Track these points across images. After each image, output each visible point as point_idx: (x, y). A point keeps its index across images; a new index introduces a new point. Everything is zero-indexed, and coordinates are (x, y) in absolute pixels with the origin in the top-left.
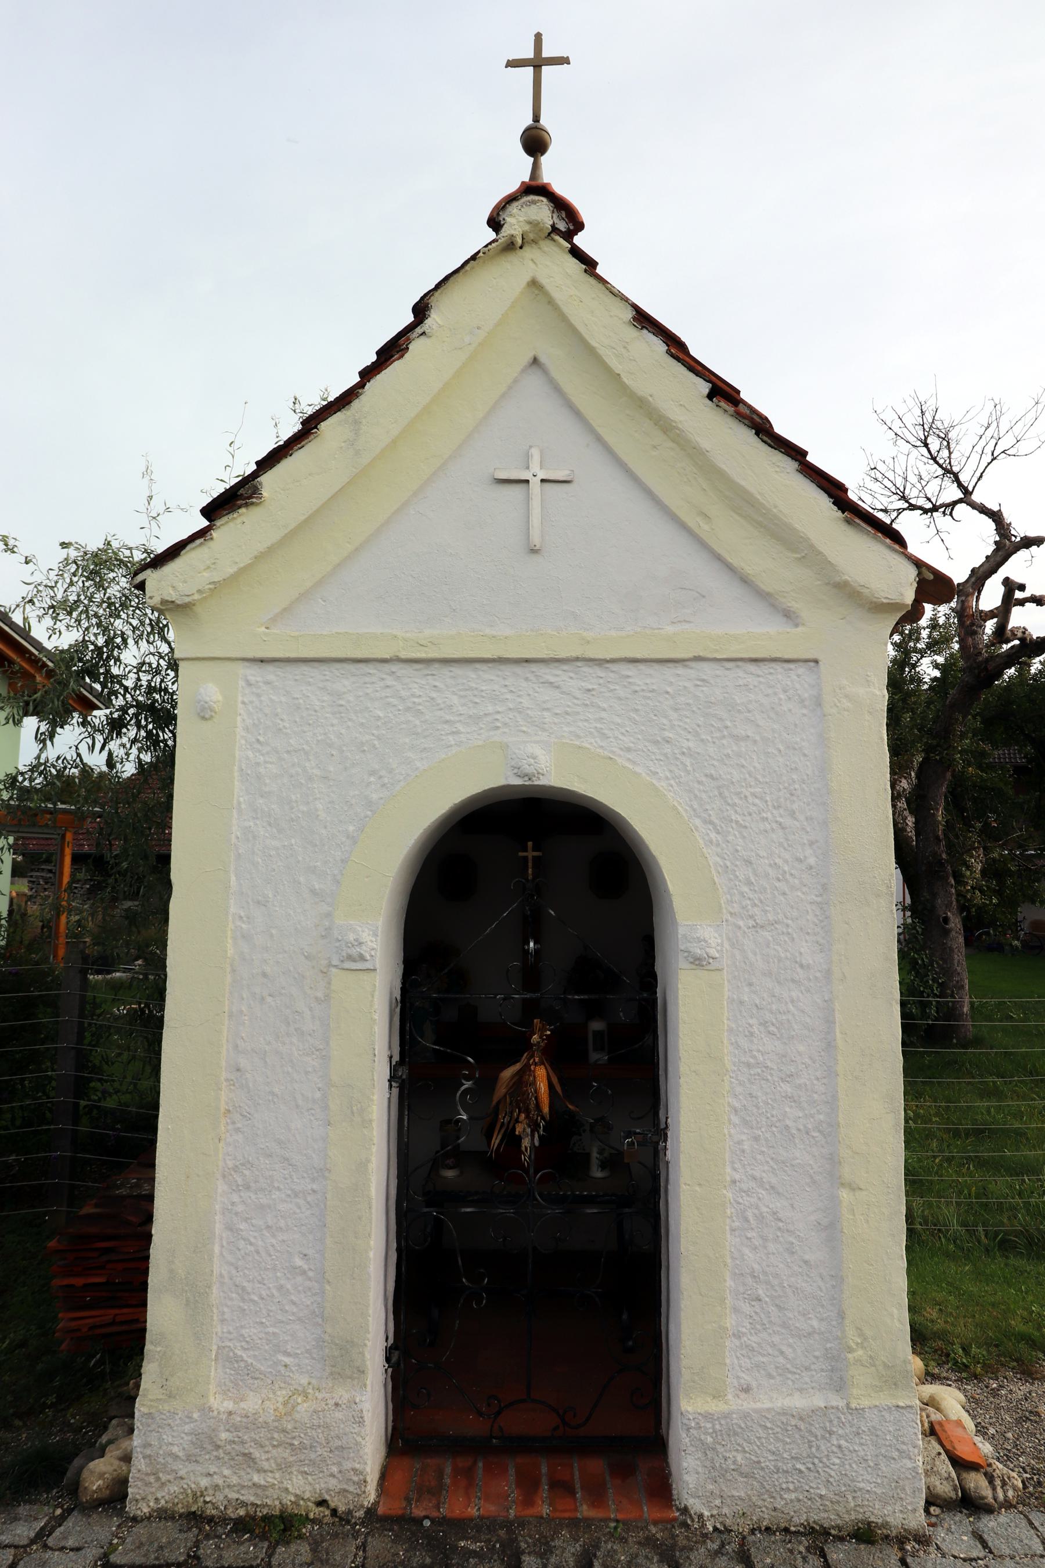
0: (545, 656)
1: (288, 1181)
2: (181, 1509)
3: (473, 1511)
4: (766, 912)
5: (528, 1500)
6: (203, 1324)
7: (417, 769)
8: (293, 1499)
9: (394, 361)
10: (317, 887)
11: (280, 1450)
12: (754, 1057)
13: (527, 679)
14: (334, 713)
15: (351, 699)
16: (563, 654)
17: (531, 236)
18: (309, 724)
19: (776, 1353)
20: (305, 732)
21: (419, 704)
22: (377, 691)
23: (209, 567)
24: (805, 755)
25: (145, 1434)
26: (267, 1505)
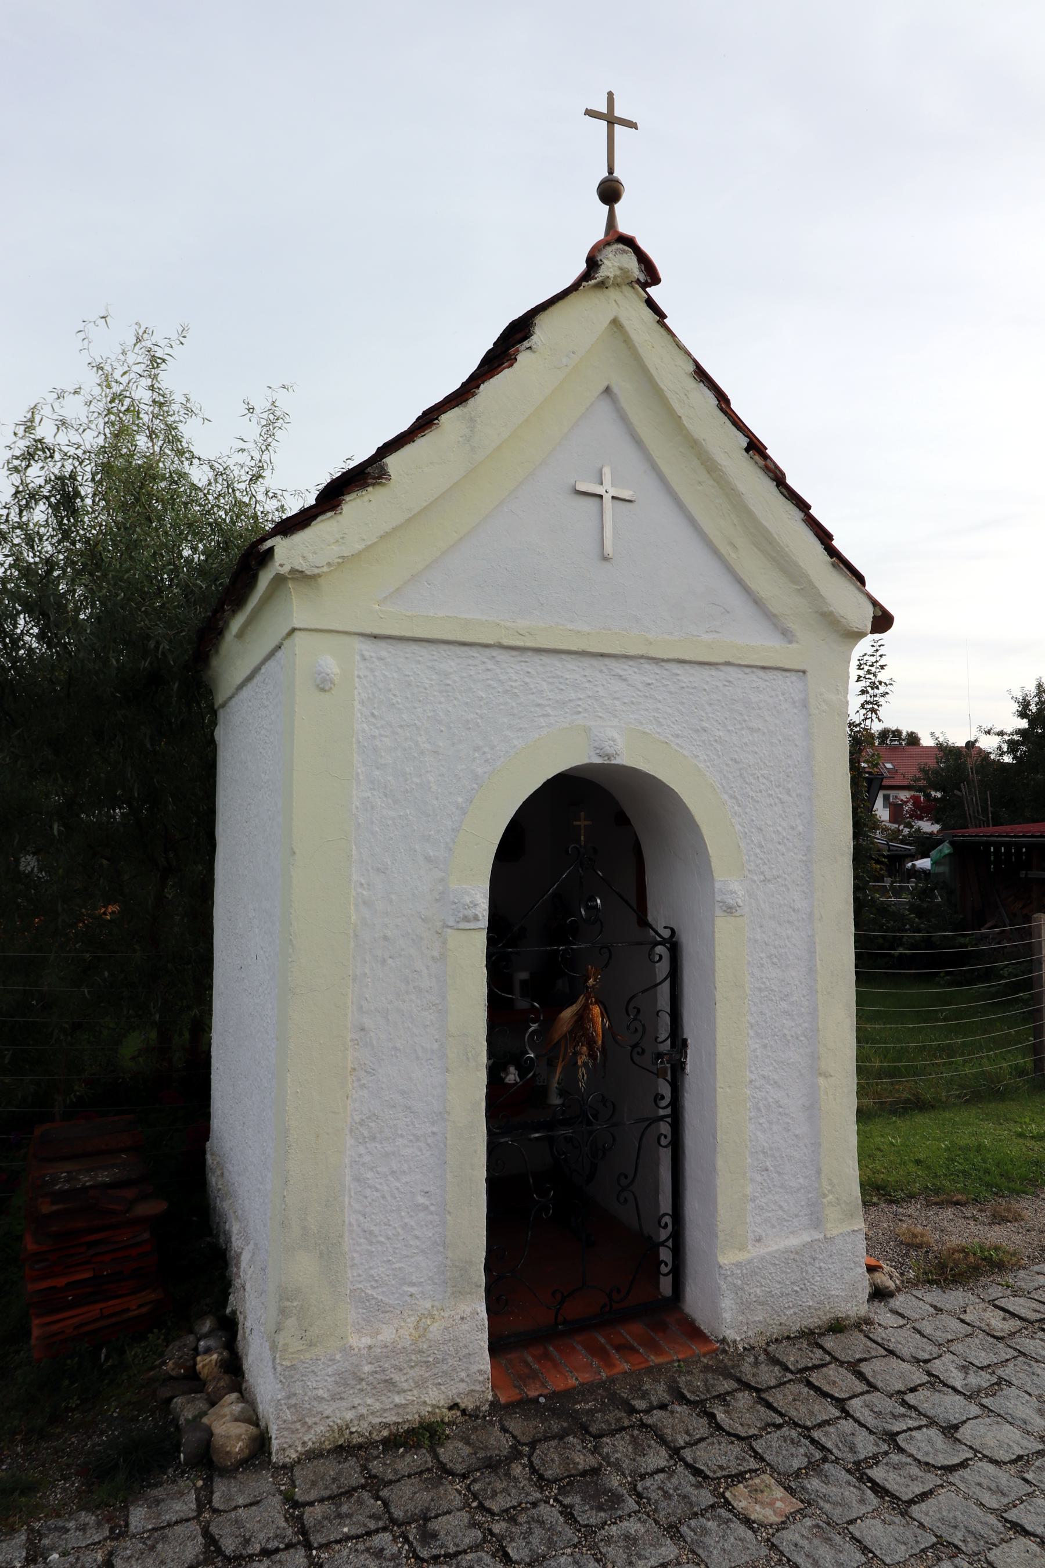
0: (618, 653)
1: (410, 1128)
2: (328, 1446)
3: (572, 1382)
4: (771, 868)
5: (609, 1364)
6: (337, 1272)
7: (515, 746)
8: (430, 1410)
9: (504, 369)
10: (432, 854)
11: (417, 1369)
12: (764, 983)
13: (601, 671)
14: (441, 692)
15: (457, 679)
16: (632, 652)
17: (619, 280)
18: (420, 701)
19: (777, 1208)
20: (415, 708)
21: (516, 688)
22: (479, 673)
23: (337, 541)
24: (796, 746)
25: (289, 1385)
26: (408, 1421)
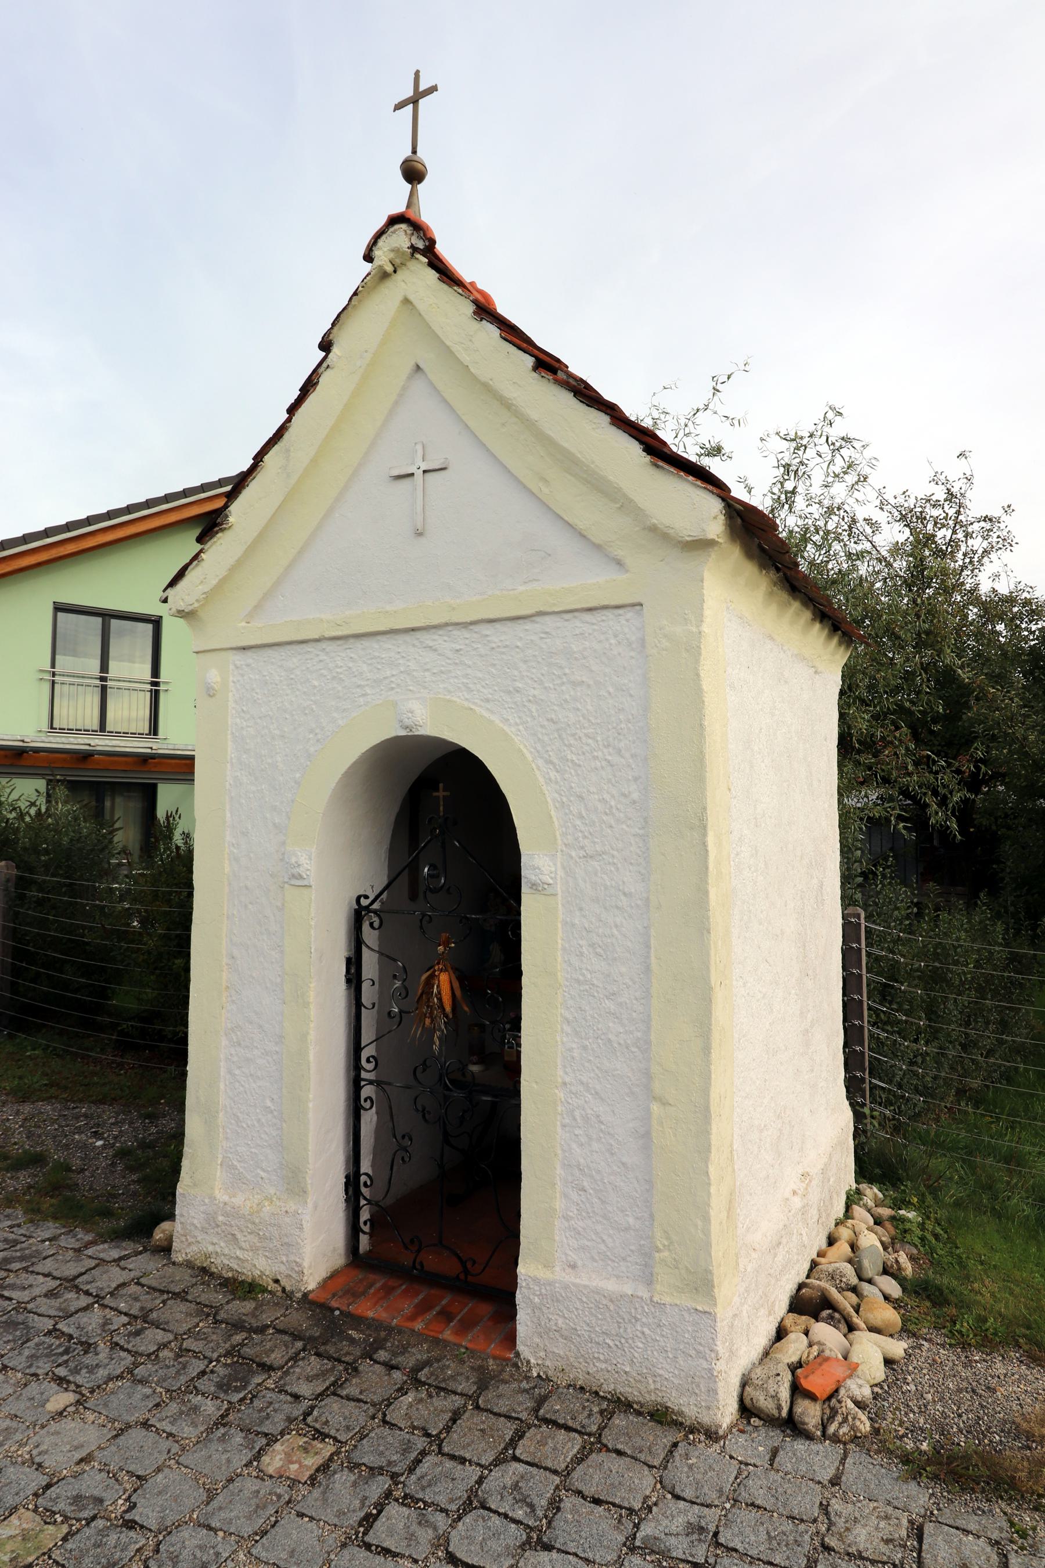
0: (423, 625)
3: (370, 1314)
4: (594, 843)
11: (252, 1236)
13: (414, 645)
15: (298, 673)
19: (599, 1240)
21: (341, 673)
24: (631, 696)
